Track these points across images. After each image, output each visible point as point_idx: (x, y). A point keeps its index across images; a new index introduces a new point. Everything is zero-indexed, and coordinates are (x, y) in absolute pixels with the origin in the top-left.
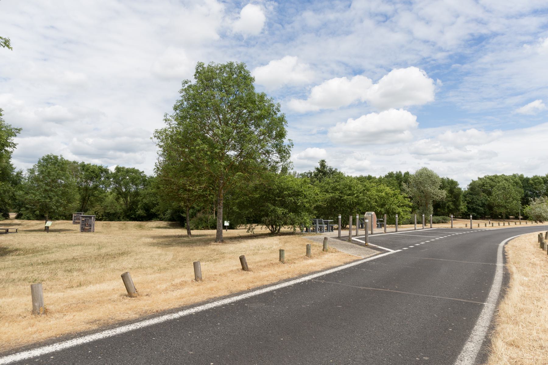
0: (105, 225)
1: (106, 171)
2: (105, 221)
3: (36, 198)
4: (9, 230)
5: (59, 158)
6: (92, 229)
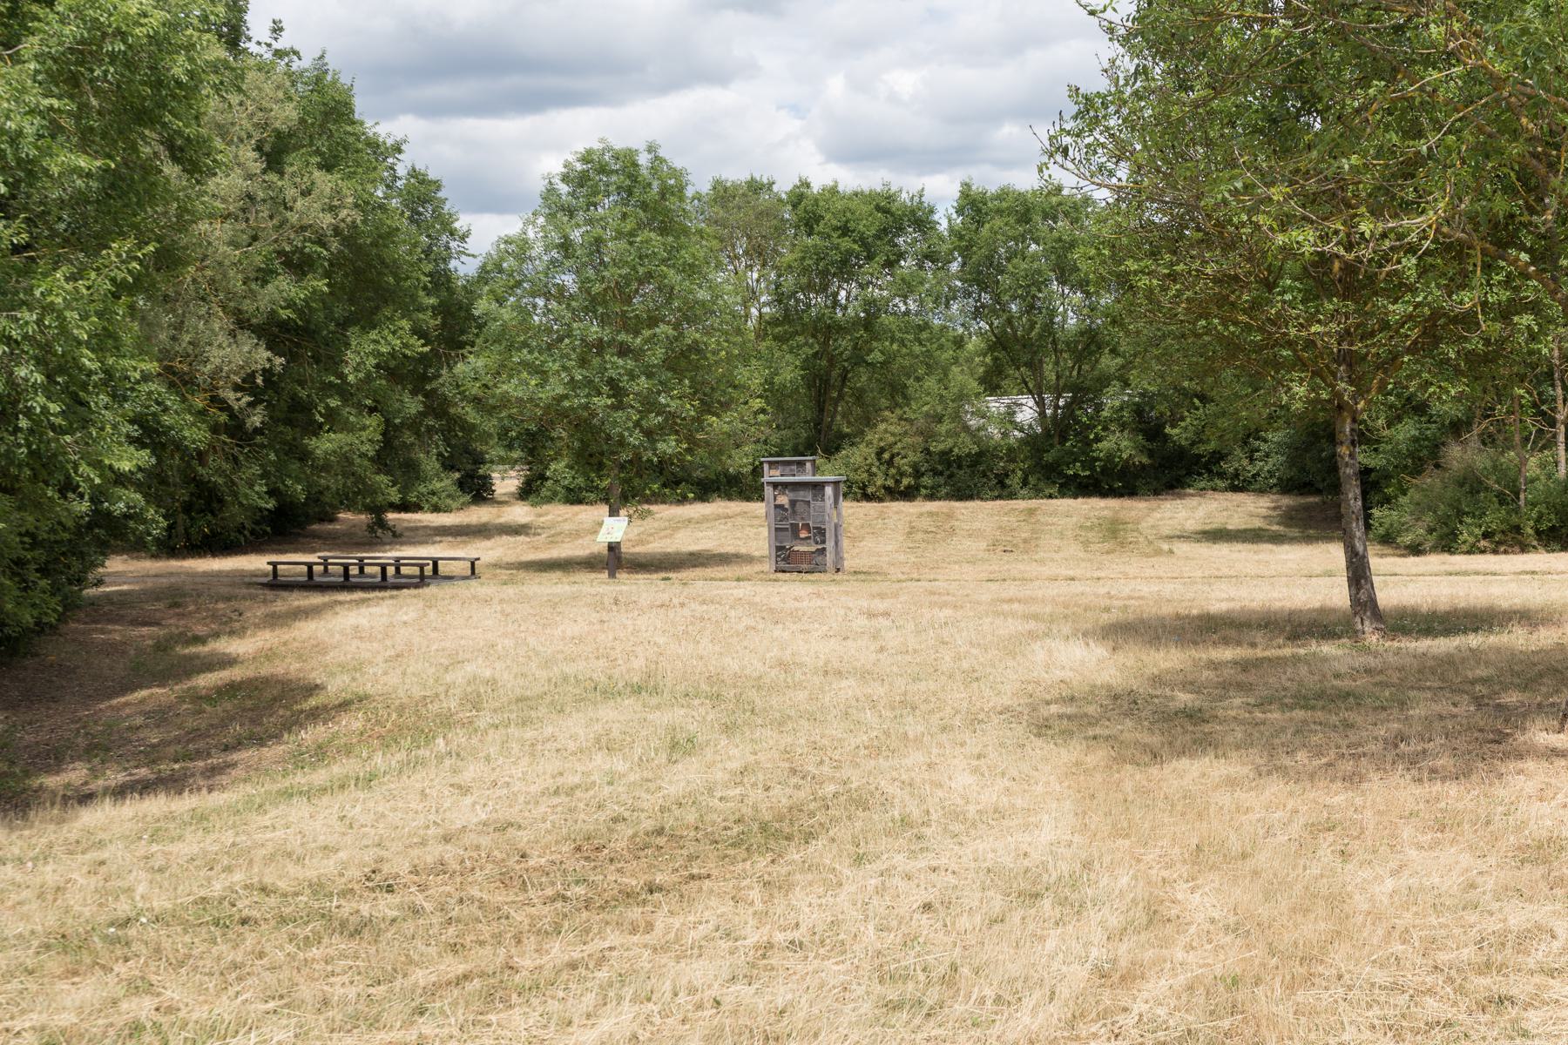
0: (925, 523)
1: (920, 218)
2: (931, 497)
3: (545, 395)
4: (443, 568)
5: (644, 160)
6: (830, 557)
